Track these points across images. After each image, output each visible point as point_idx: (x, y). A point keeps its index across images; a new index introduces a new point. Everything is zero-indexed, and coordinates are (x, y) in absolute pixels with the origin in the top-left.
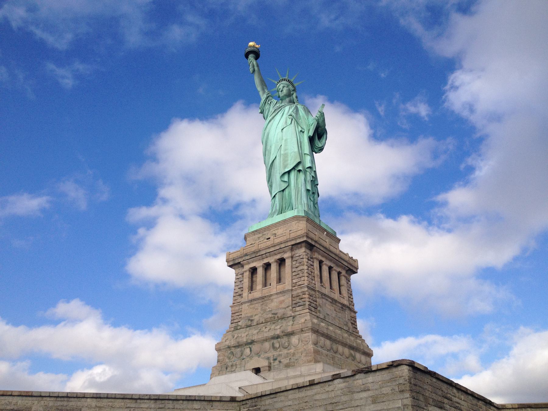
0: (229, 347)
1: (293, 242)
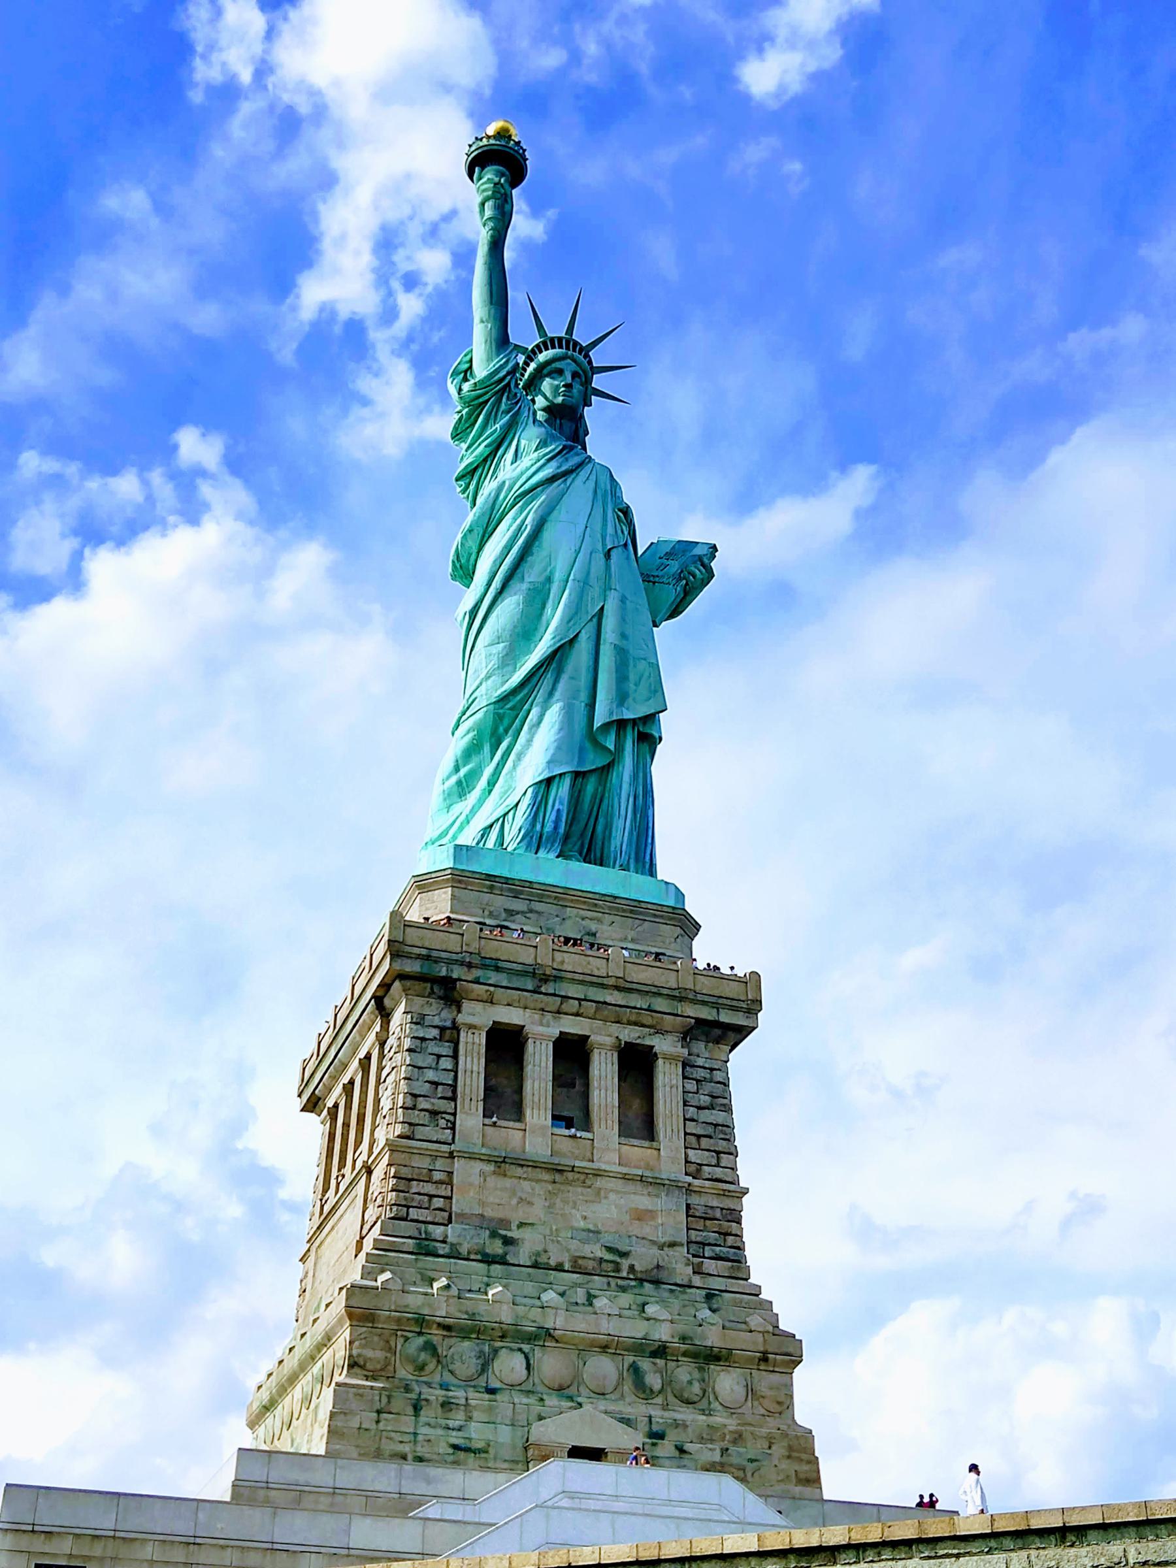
0: (421, 1322)
1: (706, 1013)
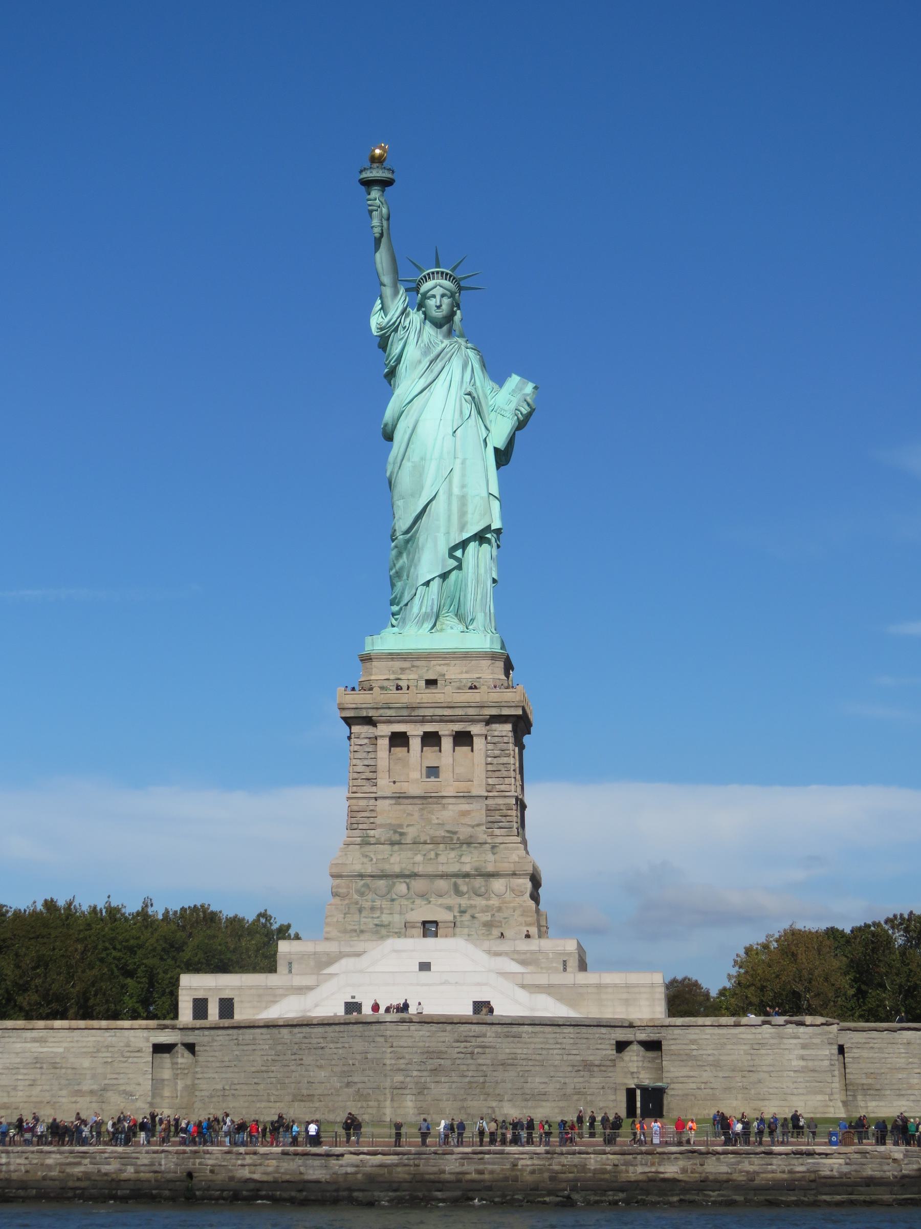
0: (361, 876)
1: (494, 712)
